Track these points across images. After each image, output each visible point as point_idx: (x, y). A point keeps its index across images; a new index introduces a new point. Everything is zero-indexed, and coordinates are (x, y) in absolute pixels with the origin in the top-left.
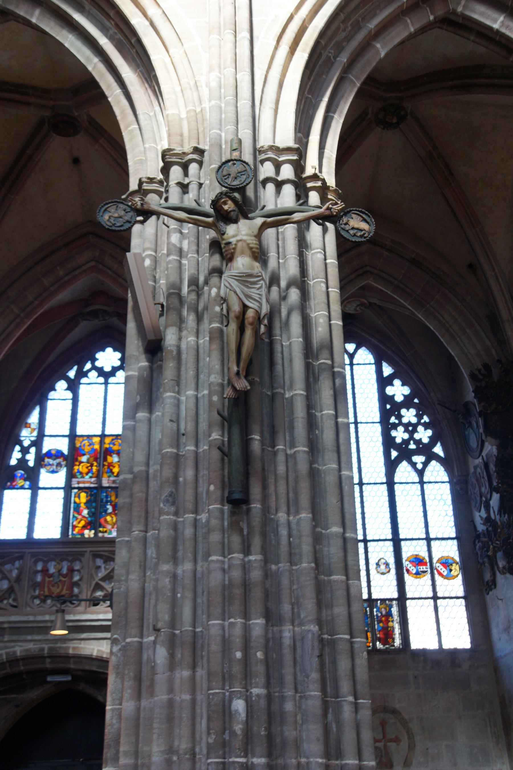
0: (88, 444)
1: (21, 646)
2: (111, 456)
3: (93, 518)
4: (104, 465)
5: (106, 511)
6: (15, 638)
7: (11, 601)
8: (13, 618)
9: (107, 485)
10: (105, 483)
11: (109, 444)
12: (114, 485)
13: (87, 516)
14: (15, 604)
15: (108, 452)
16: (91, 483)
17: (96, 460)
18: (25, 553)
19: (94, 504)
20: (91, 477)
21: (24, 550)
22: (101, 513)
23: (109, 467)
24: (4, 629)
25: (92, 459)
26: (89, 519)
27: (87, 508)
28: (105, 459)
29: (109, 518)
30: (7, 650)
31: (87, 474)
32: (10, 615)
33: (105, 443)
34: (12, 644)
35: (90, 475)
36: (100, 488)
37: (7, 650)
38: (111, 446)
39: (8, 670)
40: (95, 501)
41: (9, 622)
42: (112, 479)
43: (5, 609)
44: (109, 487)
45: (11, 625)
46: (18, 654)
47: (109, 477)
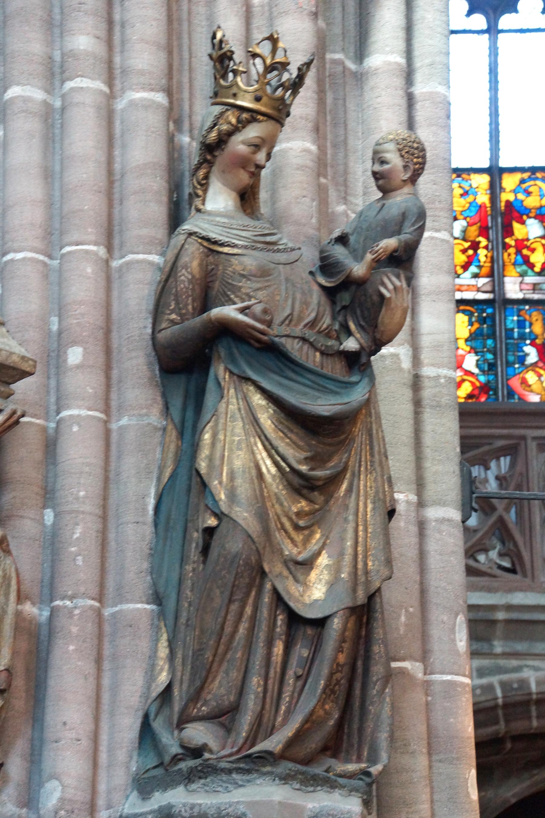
0: (458, 191)
1: (536, 669)
2: (523, 223)
3: (491, 378)
4: (506, 246)
5: (522, 360)
6: (520, 647)
7: (493, 554)
8: (519, 598)
9: (520, 296)
10: (513, 289)
11: (514, 191)
12: (536, 297)
13: (476, 371)
14: (506, 564)
15: (513, 214)
16: (478, 290)
17: (484, 231)
18: (523, 438)
19: (490, 342)
20: (476, 276)
21: (522, 432)
22: (509, 364)
23: (519, 252)
24: (494, 622)
25: (473, 231)
26: (482, 379)
27: (474, 350)
28: (508, 231)
29: (531, 377)
30: (505, 677)
31: (465, 267)
32: (510, 590)
33: (502, 189)
34: (514, 663)
35: (473, 269)
36: (501, 302)
37: (505, 677)
38: (521, 196)
39: (502, 727)
40: (492, 335)
41: (509, 608)
42: (531, 279)
43: (494, 576)
44: (525, 301)
45: (515, 615)
46: (534, 688)
47: (522, 275)
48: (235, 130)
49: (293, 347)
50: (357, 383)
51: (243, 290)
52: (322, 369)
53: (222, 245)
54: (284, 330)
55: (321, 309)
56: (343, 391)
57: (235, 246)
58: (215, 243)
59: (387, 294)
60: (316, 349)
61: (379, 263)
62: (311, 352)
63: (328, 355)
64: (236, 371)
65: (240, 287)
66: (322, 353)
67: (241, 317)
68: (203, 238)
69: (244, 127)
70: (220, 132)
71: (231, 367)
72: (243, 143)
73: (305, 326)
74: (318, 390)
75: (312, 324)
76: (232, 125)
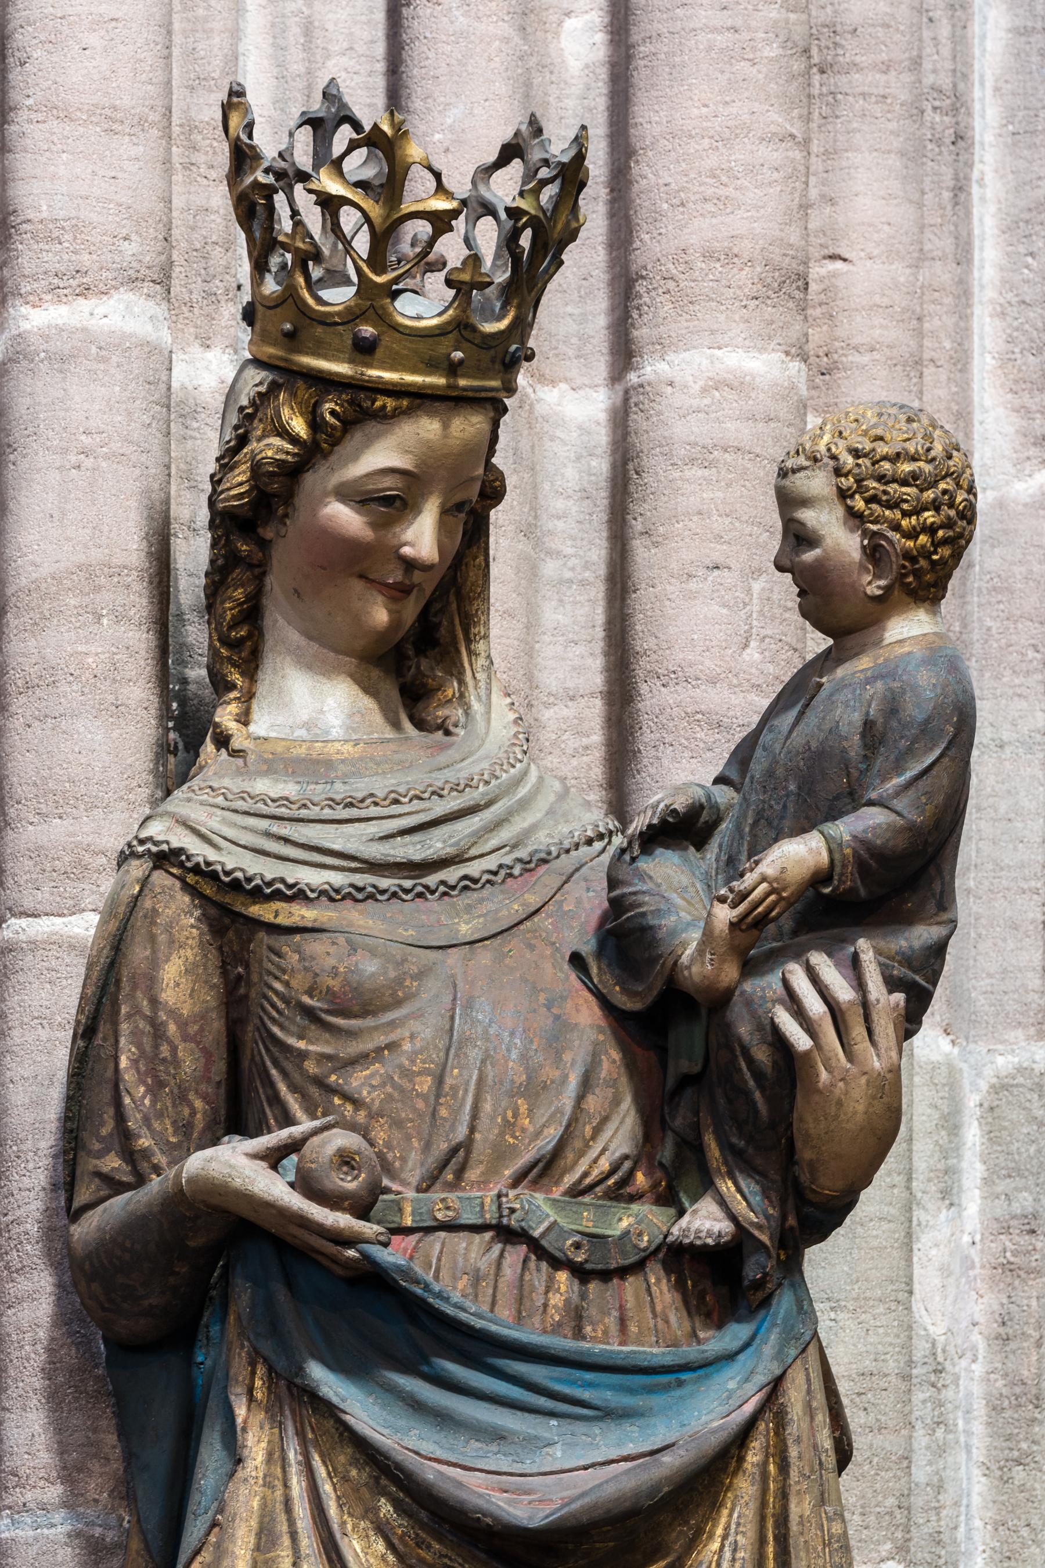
48: (314, 451)
49: (459, 1274)
50: (730, 1357)
51: (311, 1067)
52: (578, 1333)
53: (258, 894)
54: (443, 1203)
55: (593, 1103)
56: (656, 1401)
57: (299, 895)
58: (236, 886)
59: (801, 1041)
60: (557, 1263)
61: (766, 935)
62: (539, 1273)
63: (605, 1276)
64: (281, 1365)
65: (303, 1055)
66: (581, 1274)
67: (276, 1188)
68: (196, 870)
69: (336, 442)
70: (256, 468)
71: (267, 1347)
72: (347, 494)
73: (516, 1182)
74: (552, 1414)
75: (542, 1171)
76: (294, 440)
